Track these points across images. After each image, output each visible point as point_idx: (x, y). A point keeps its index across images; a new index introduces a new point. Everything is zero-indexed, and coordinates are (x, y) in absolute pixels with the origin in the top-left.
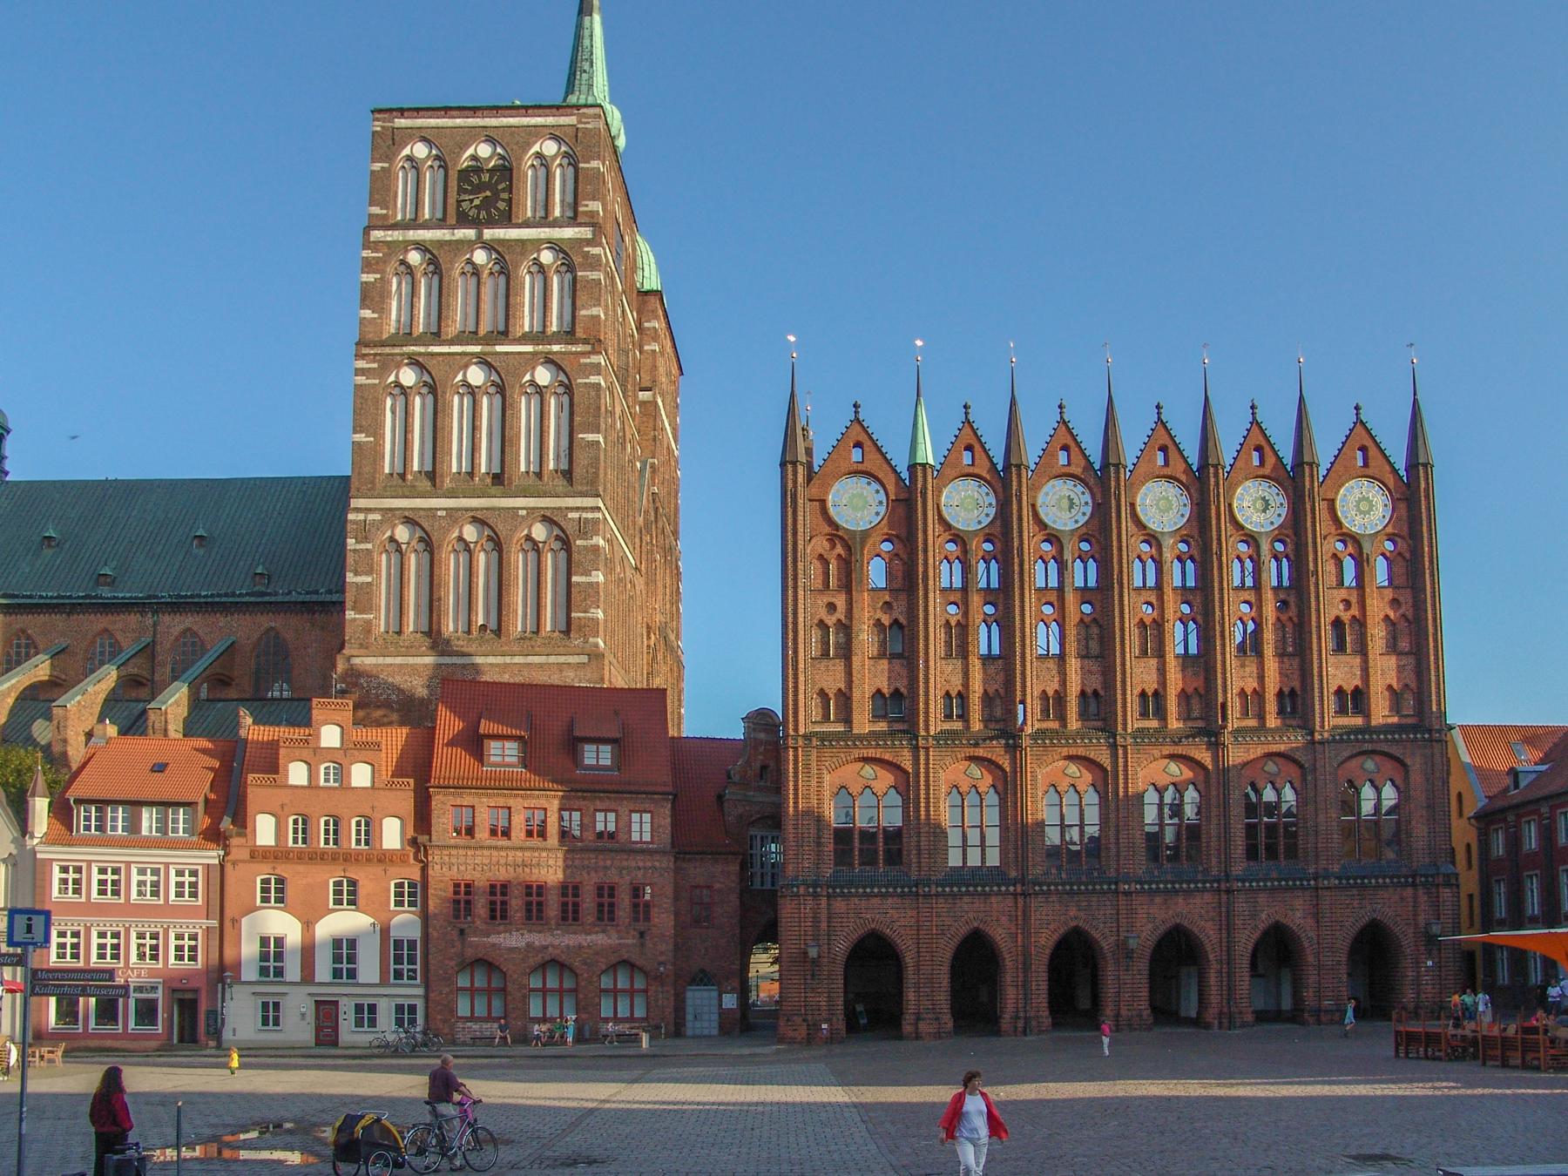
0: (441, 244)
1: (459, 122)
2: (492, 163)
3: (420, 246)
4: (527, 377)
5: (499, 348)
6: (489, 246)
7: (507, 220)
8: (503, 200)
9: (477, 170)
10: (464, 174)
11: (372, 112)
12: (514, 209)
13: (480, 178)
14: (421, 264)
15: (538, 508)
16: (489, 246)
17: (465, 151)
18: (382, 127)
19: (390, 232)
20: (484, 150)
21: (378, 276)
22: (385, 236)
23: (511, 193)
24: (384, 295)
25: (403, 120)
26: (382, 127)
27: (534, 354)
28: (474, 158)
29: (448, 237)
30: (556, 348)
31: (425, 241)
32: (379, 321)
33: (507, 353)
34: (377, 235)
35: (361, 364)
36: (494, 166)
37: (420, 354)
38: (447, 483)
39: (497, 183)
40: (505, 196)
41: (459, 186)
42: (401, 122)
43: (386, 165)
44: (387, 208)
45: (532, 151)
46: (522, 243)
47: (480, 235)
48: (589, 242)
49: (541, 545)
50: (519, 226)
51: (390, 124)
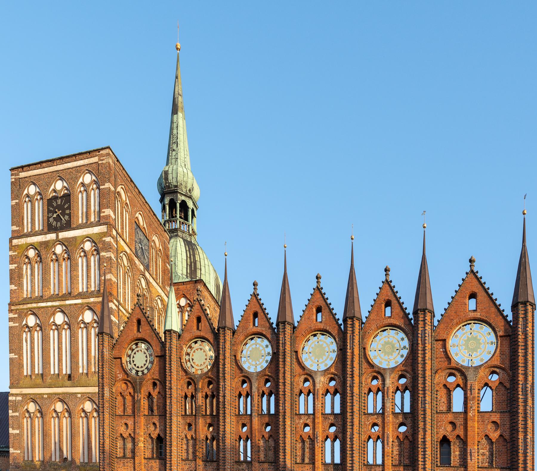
0: (41, 243)
1: (47, 170)
2: (62, 193)
3: (33, 246)
4: (80, 318)
5: (68, 302)
6: (62, 242)
7: (68, 226)
8: (67, 214)
9: (55, 198)
10: (50, 201)
11: (10, 170)
12: (72, 219)
13: (57, 203)
14: (34, 257)
15: (86, 393)
16: (62, 242)
17: (50, 187)
18: (15, 179)
19: (20, 240)
20: (59, 185)
21: (16, 265)
22: (19, 242)
23: (70, 210)
24: (20, 276)
25: (23, 173)
26: (15, 179)
27: (82, 304)
28: (55, 191)
29: (44, 240)
30: (92, 300)
31: (34, 243)
32: (17, 291)
33: (70, 305)
34: (15, 242)
35: (12, 315)
36: (64, 194)
37: (34, 308)
38: (49, 380)
39: (64, 204)
40: (67, 212)
41: (48, 209)
42: (23, 175)
43: (17, 201)
44: (19, 226)
45: (79, 183)
46: (75, 238)
47: (57, 236)
48: (104, 234)
49: (88, 414)
50: (74, 229)
51: (18, 177)
